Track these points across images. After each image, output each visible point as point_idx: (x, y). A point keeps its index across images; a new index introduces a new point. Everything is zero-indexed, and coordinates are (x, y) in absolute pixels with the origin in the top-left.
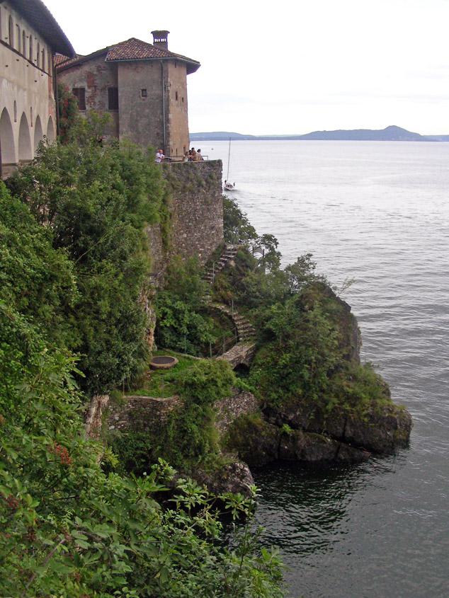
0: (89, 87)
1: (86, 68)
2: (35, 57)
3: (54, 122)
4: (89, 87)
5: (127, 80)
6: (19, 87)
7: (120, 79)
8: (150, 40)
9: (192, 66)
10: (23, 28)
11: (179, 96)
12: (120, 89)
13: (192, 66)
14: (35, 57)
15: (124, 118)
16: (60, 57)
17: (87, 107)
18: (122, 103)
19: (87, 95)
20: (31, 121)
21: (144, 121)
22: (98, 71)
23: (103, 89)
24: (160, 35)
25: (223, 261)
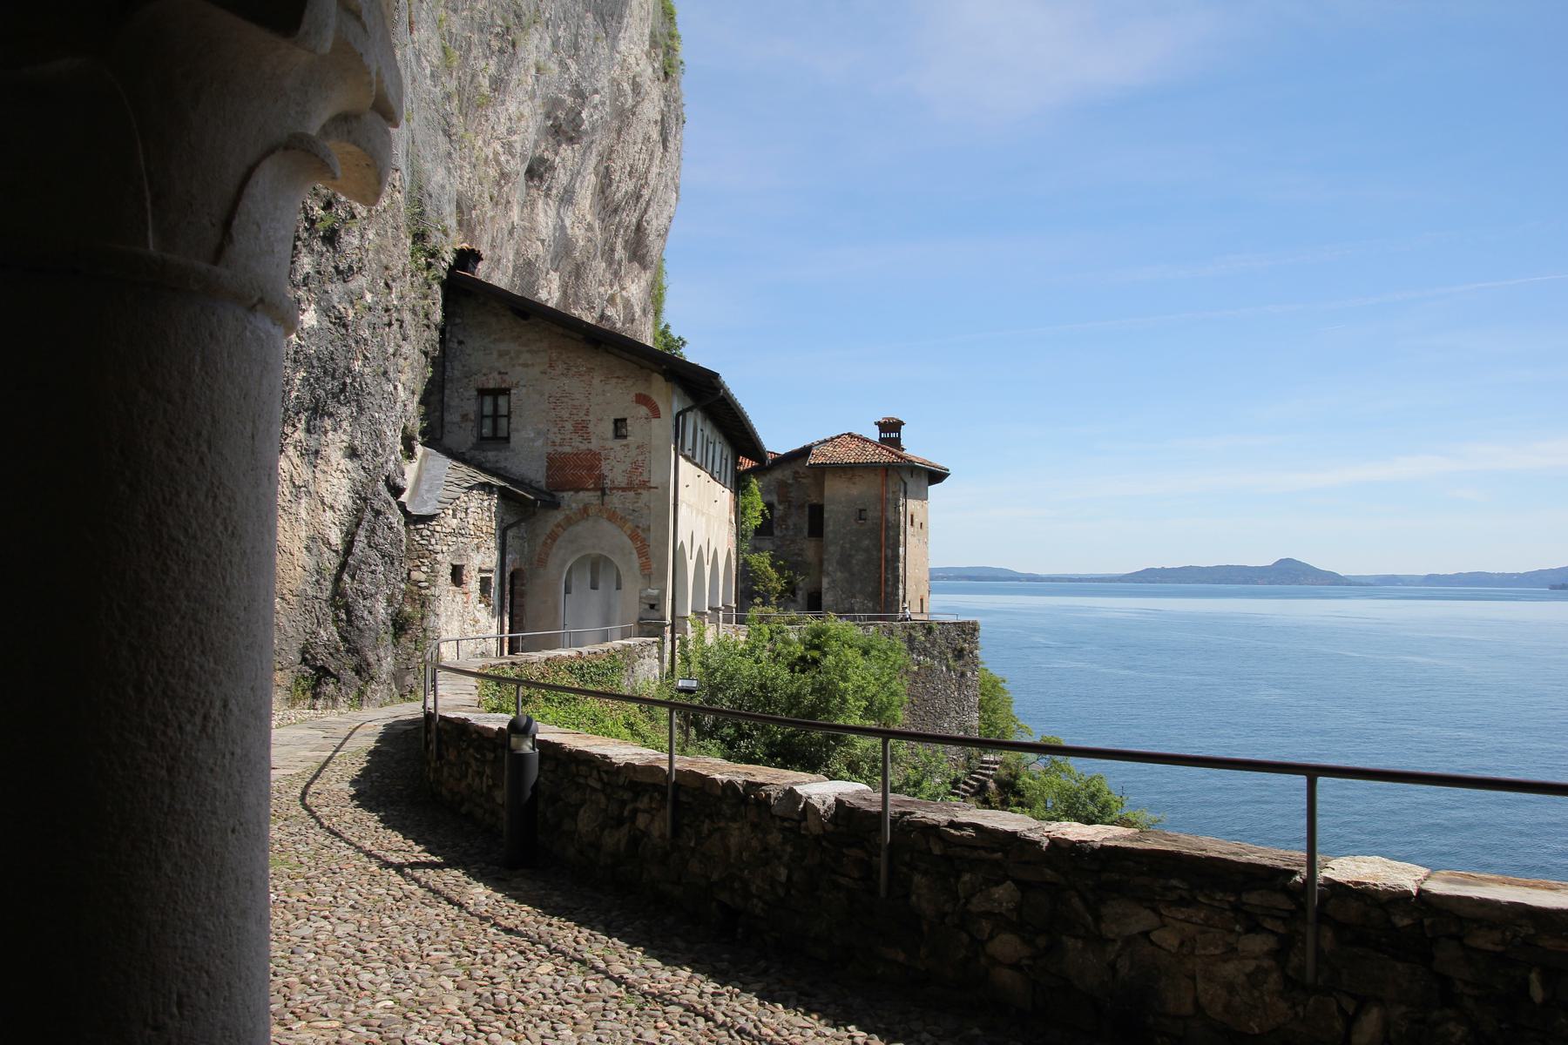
0: (780, 502)
1: (778, 474)
2: (717, 468)
3: (733, 556)
4: (780, 502)
5: (837, 493)
6: (698, 511)
7: (826, 493)
8: (874, 434)
9: (936, 476)
10: (707, 432)
11: (916, 520)
12: (827, 508)
13: (936, 476)
14: (717, 468)
15: (833, 551)
16: (747, 464)
17: (776, 532)
18: (830, 528)
19: (777, 514)
20: (707, 559)
21: (861, 557)
22: (795, 478)
23: (801, 507)
24: (891, 429)
25: (977, 780)
